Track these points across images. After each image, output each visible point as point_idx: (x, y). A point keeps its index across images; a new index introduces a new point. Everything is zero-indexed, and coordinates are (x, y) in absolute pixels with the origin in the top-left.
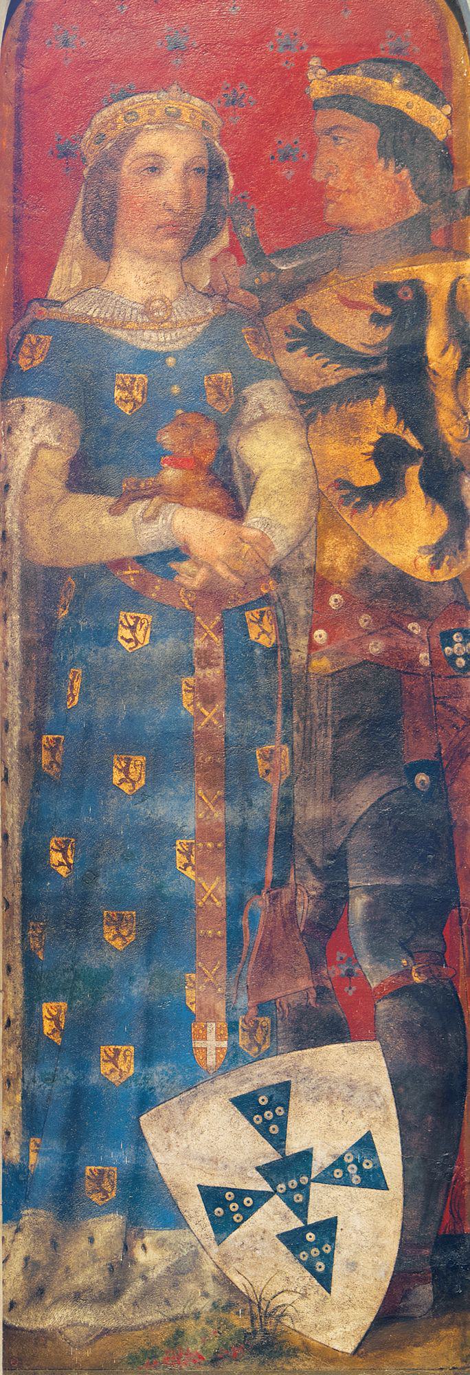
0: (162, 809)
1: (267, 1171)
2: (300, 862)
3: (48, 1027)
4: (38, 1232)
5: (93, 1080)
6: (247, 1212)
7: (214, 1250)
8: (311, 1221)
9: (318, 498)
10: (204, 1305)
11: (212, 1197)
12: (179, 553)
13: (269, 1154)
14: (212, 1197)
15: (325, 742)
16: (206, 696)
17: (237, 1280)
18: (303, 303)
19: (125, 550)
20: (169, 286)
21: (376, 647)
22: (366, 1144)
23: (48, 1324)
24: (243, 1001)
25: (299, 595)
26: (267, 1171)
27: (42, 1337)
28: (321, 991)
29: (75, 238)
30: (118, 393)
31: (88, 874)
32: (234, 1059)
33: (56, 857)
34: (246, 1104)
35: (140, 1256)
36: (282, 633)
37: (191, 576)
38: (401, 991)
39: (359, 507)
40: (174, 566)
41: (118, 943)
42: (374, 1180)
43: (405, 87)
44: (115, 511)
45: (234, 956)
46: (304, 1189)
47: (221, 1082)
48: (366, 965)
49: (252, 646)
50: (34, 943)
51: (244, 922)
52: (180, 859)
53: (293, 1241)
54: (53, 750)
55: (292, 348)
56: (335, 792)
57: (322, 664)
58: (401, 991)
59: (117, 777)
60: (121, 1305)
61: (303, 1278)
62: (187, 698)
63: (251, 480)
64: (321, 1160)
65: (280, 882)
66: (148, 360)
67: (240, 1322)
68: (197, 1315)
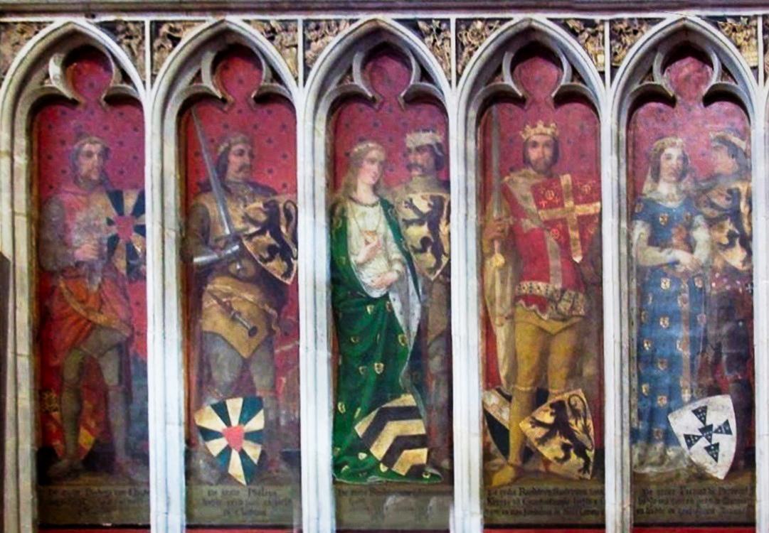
0: (673, 332)
1: (702, 430)
2: (709, 346)
3: (644, 391)
4: (642, 447)
5: (656, 406)
6: (696, 441)
7: (688, 452)
8: (713, 442)
9: (713, 248)
10: (685, 466)
11: (687, 437)
12: (677, 262)
13: (701, 425)
14: (687, 437)
15: (715, 313)
16: (684, 301)
17: (694, 459)
18: (709, 194)
19: (663, 262)
20: (674, 190)
21: (728, 288)
22: (727, 423)
23: (643, 472)
24: (695, 384)
25: (708, 273)
26: (702, 430)
27: (644, 475)
28: (715, 381)
29: (649, 177)
30: (661, 219)
31: (654, 350)
32: (692, 400)
33: (646, 345)
34: (696, 412)
35: (669, 453)
36: (704, 282)
37: (680, 269)
38: (737, 381)
39: (724, 250)
40: (677, 266)
41: (662, 369)
42: (729, 432)
43: (735, 136)
44: (661, 251)
45: (692, 372)
46: (711, 435)
47: (688, 406)
48: (726, 373)
49: (696, 287)
50: (641, 369)
51: (695, 362)
52: (678, 346)
53: (708, 449)
54: (645, 316)
55: (705, 206)
56: (718, 328)
57: (714, 292)
58: (737, 381)
59: (661, 323)
60: (664, 467)
61: (710, 458)
62: (679, 302)
63: (695, 242)
64: (715, 427)
65: (704, 351)
66: (669, 210)
67: (694, 471)
68: (683, 469)
